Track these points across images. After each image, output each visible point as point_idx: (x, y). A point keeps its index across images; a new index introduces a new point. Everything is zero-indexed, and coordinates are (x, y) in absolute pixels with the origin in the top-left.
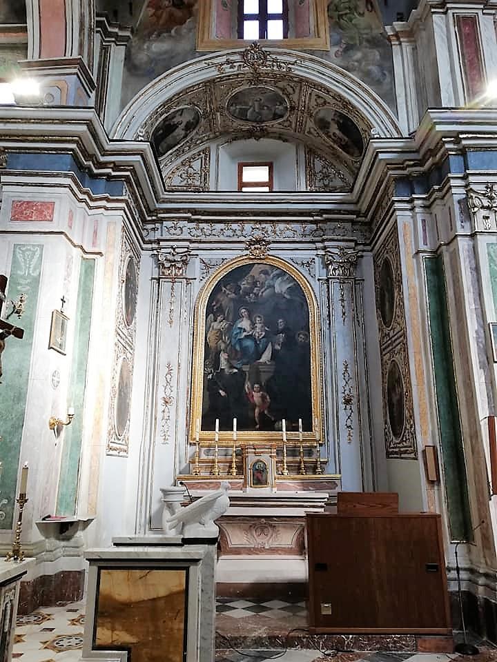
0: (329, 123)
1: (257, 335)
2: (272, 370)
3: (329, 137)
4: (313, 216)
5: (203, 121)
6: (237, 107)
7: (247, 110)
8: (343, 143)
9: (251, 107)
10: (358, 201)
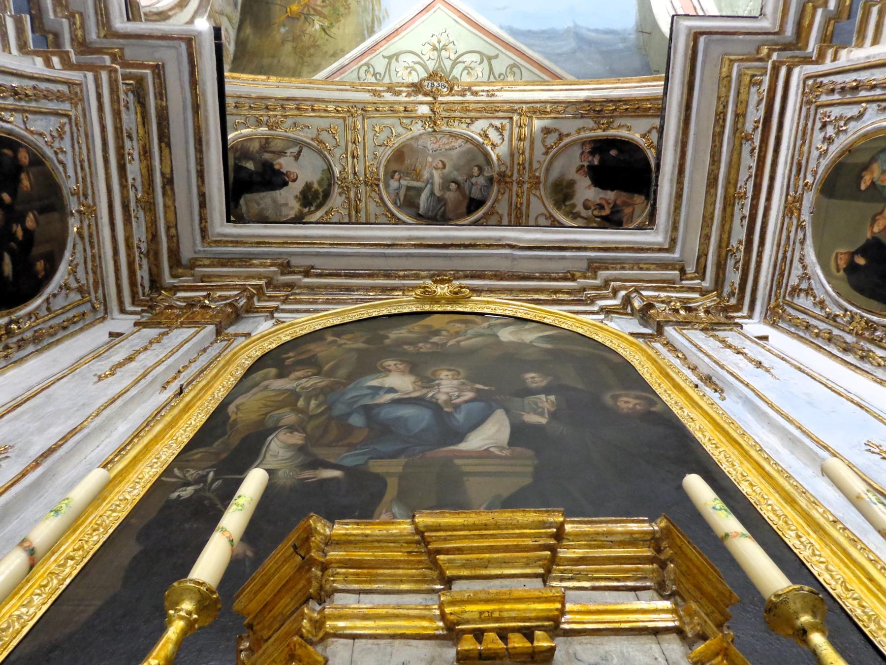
0: (571, 184)
1: (442, 398)
2: (531, 469)
4: (573, 279)
6: (403, 182)
7: (419, 191)
8: (606, 212)
10: (673, 241)
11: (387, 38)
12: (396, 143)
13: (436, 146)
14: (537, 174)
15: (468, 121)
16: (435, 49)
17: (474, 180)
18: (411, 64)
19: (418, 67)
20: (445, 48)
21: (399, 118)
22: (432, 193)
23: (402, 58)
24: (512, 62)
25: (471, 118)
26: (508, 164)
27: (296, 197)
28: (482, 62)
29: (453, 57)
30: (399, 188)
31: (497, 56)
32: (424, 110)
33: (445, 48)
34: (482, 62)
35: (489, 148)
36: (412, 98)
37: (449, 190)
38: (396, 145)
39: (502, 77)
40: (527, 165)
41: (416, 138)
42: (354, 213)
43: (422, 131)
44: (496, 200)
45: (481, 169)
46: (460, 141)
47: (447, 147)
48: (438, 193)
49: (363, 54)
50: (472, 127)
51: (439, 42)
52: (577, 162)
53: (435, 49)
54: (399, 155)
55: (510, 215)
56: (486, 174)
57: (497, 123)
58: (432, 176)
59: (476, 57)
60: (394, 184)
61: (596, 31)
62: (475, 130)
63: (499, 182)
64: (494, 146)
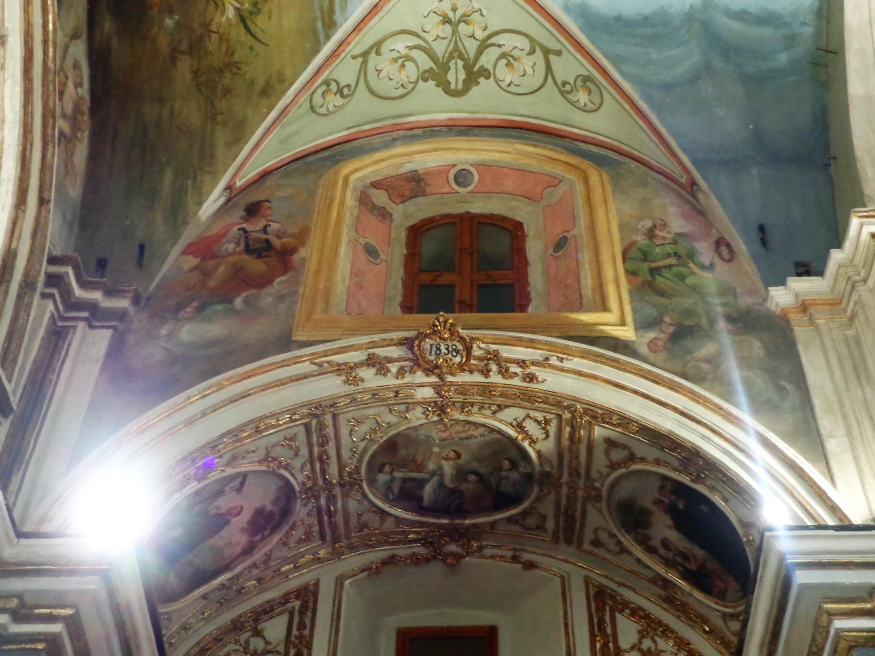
3: (651, 550)
5: (301, 511)
6: (397, 474)
7: (422, 483)
8: (692, 566)
9: (433, 474)
11: (358, 28)
12: (382, 438)
13: (443, 435)
14: (597, 485)
15: (494, 408)
16: (446, 20)
17: (504, 474)
18: (404, 51)
19: (417, 54)
20: (465, 19)
21: (388, 405)
22: (441, 484)
23: (385, 48)
24: (586, 73)
25: (499, 406)
26: (555, 461)
27: (243, 529)
28: (532, 52)
29: (480, 35)
30: (392, 480)
31: (559, 53)
32: (428, 393)
33: (465, 19)
34: (532, 52)
35: (526, 444)
36: (408, 379)
37: (468, 482)
38: (385, 439)
39: (568, 88)
40: (582, 471)
41: (416, 428)
42: (326, 518)
43: (423, 421)
44: (538, 499)
45: (514, 465)
46: (481, 430)
47: (463, 435)
48: (448, 483)
49: (317, 73)
50: (499, 415)
51: (454, 9)
52: (656, 495)
53: (446, 20)
54: (391, 446)
55: (557, 517)
56: (521, 469)
57: (540, 416)
58: (440, 468)
59: (523, 43)
60: (383, 478)
61: (742, 16)
62: (504, 422)
63: (541, 483)
64: (533, 442)
